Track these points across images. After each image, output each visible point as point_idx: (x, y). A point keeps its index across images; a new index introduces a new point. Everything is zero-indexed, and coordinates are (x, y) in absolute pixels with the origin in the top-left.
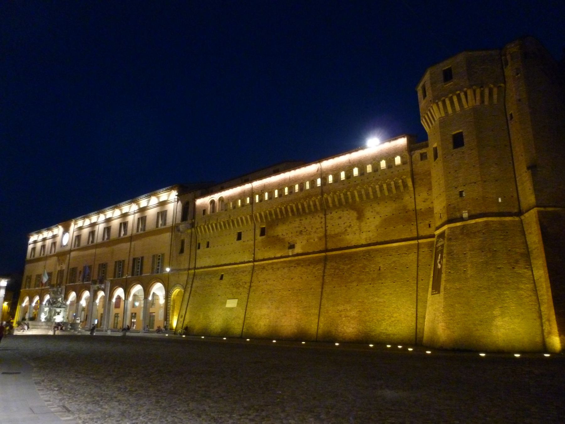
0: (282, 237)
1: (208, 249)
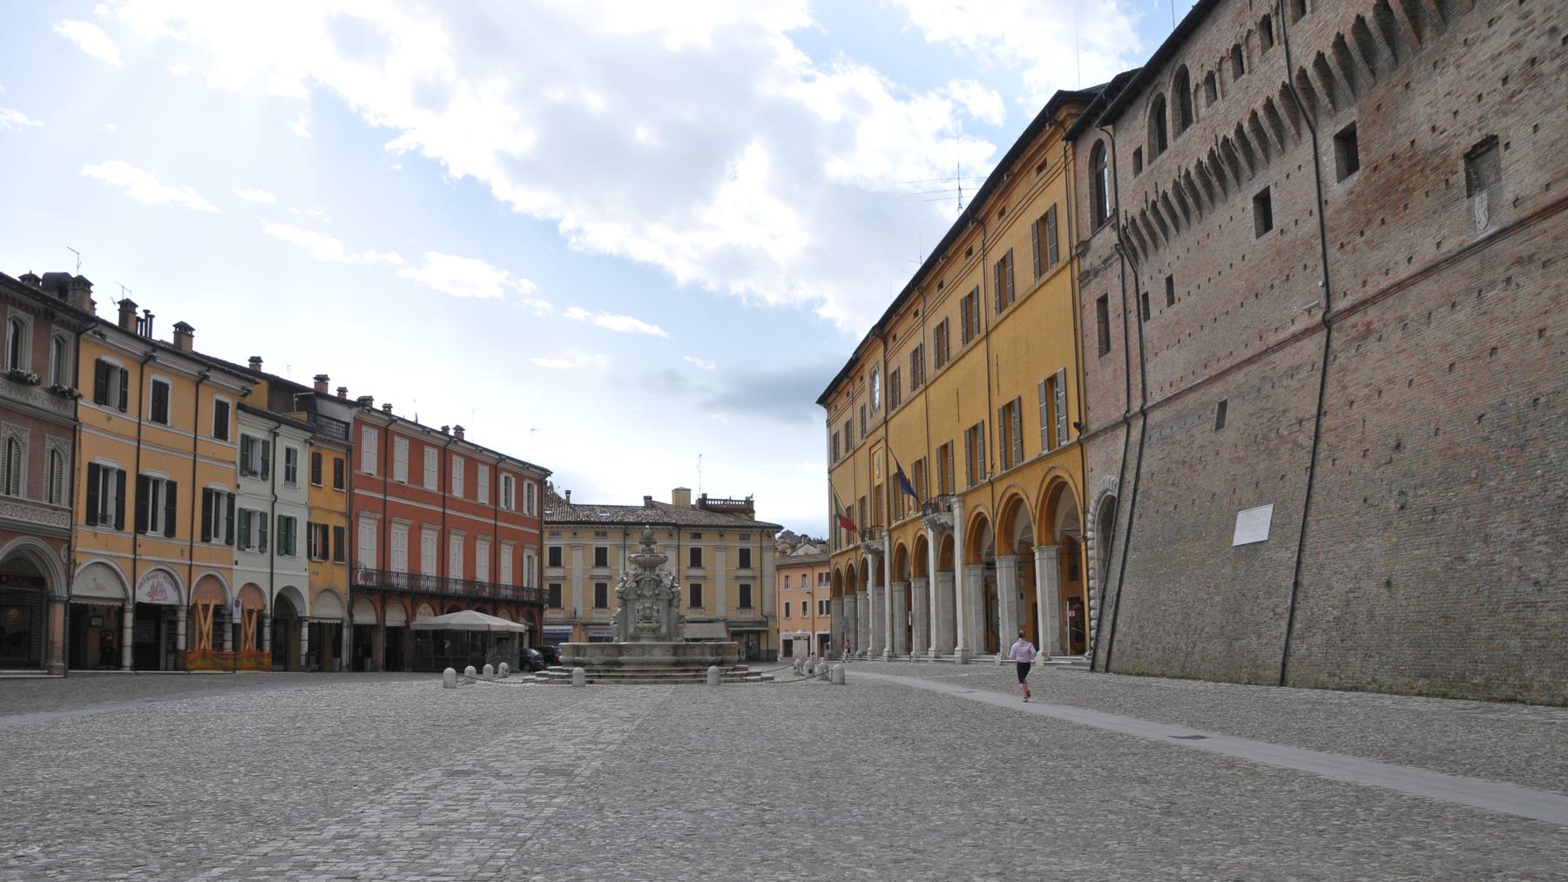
0: (1427, 142)
1: (1176, 307)
